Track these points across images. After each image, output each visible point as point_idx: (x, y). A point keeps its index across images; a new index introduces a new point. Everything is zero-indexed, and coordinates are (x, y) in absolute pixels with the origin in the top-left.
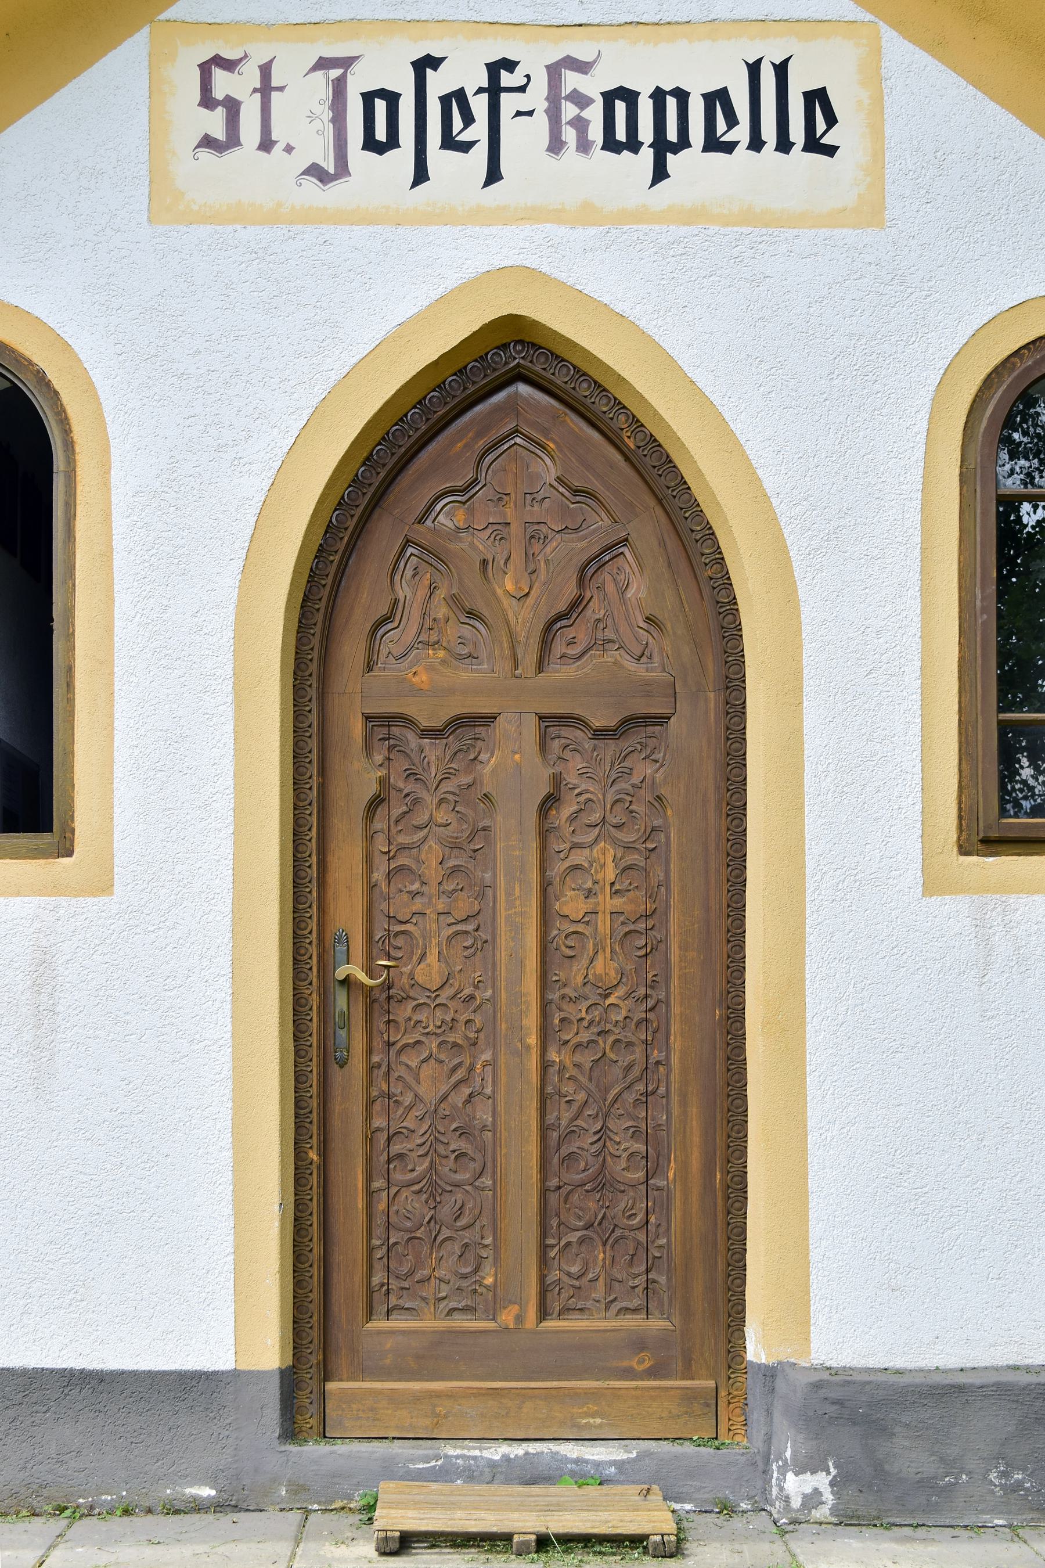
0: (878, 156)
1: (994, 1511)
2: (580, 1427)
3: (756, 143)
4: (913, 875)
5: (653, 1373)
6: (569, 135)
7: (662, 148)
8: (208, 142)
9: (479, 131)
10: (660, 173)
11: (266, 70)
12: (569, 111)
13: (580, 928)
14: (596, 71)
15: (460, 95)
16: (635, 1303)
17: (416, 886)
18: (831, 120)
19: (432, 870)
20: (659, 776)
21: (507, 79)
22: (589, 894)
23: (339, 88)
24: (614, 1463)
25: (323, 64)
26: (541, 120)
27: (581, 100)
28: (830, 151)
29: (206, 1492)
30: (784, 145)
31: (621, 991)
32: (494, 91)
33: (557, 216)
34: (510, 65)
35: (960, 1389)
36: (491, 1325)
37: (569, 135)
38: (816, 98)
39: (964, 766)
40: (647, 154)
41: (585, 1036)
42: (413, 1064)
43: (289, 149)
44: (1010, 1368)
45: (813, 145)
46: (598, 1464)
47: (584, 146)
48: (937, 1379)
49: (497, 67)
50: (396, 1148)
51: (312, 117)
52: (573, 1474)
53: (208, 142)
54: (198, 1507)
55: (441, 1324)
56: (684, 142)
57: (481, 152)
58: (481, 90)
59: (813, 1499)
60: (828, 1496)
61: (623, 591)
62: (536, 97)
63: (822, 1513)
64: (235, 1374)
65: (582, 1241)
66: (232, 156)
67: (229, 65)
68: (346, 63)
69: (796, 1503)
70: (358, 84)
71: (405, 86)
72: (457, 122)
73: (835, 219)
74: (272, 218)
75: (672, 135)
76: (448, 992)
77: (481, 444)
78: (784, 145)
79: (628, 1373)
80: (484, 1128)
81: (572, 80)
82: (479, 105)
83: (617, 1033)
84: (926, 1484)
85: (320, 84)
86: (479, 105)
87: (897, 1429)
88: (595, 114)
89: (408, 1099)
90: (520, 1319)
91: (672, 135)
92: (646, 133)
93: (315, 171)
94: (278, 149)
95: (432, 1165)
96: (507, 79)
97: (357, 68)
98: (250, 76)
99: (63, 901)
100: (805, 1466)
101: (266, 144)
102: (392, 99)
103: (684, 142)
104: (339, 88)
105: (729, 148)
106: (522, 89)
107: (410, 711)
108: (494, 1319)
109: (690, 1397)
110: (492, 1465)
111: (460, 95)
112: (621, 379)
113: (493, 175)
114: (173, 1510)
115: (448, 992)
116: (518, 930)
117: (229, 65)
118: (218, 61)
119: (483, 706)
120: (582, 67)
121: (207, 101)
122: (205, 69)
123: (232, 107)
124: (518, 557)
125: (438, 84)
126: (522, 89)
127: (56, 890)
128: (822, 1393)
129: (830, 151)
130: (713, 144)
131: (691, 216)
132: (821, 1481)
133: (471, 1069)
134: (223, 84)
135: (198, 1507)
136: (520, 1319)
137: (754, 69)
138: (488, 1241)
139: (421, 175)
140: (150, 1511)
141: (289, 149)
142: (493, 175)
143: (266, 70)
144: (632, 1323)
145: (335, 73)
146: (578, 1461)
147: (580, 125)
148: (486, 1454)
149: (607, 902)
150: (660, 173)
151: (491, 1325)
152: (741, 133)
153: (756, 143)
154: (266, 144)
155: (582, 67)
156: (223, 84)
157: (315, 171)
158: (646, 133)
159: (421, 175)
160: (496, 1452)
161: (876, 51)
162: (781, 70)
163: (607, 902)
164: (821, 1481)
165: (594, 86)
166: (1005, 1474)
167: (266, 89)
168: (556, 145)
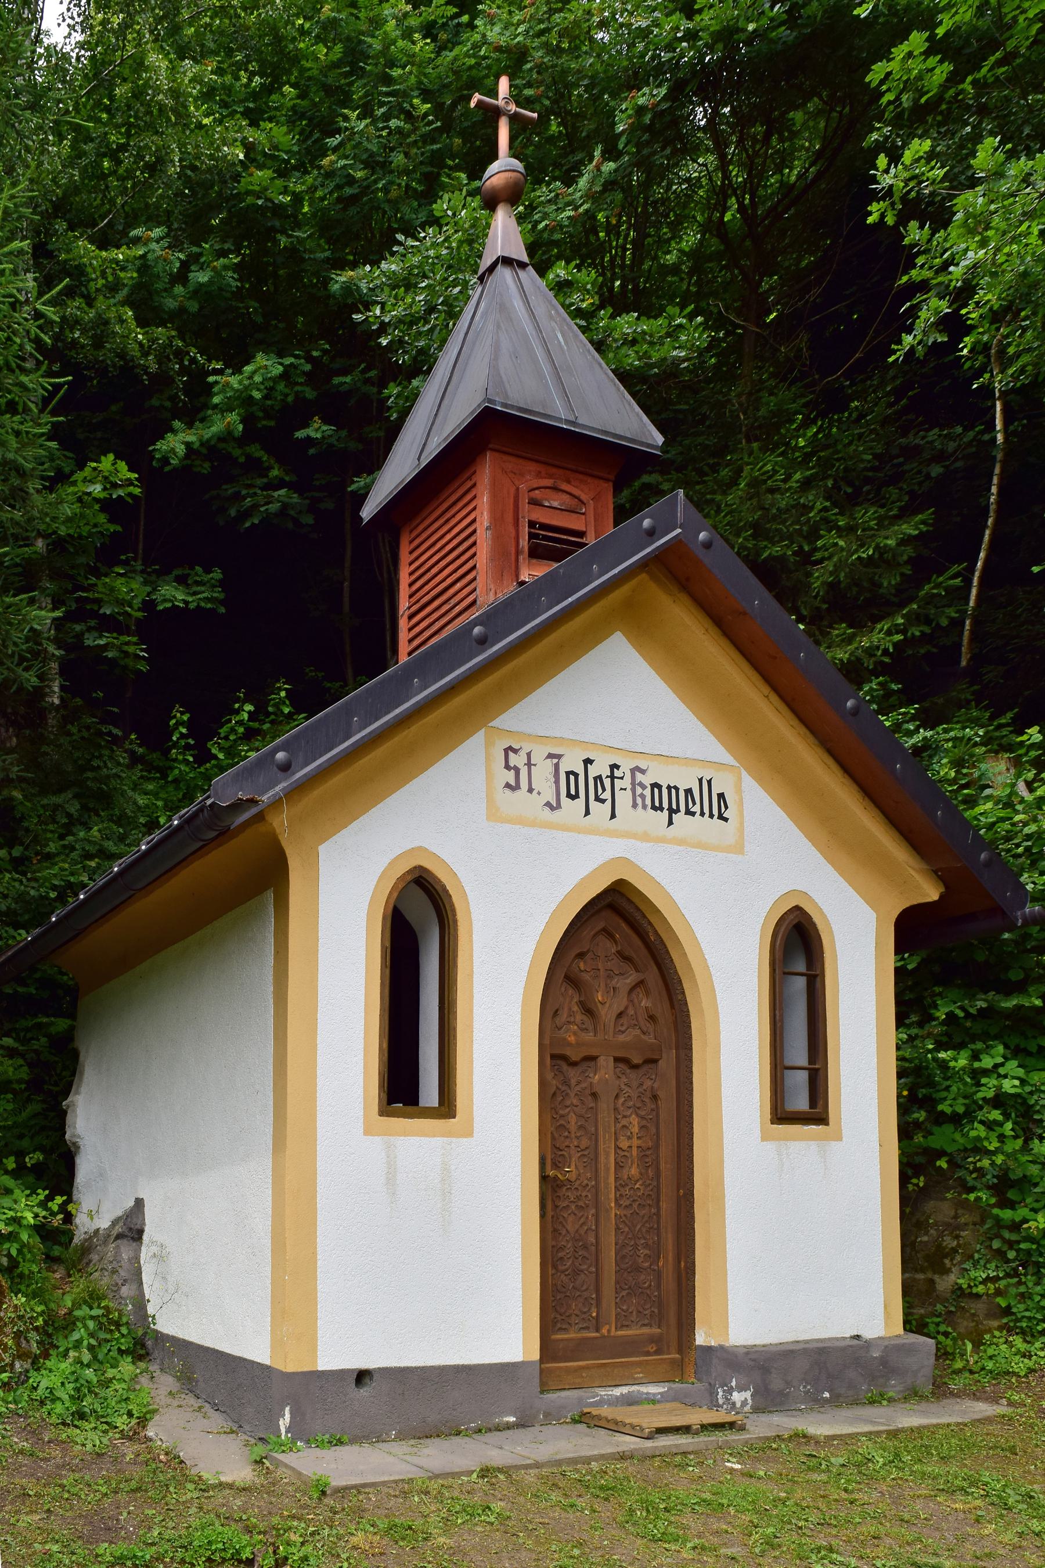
0: (742, 823)
1: (802, 1403)
2: (635, 1379)
3: (702, 814)
4: (757, 1132)
5: (658, 1352)
6: (639, 801)
7: (672, 811)
8: (508, 786)
9: (607, 795)
10: (670, 823)
11: (529, 755)
12: (639, 790)
13: (626, 1153)
14: (648, 773)
15: (600, 777)
16: (646, 1322)
17: (566, 1134)
18: (726, 807)
19: (573, 1126)
20: (656, 1085)
21: (617, 773)
22: (629, 1138)
23: (557, 767)
24: (659, 1393)
25: (550, 756)
26: (629, 792)
27: (641, 785)
28: (726, 820)
29: (512, 1419)
30: (711, 816)
31: (640, 1182)
32: (612, 777)
33: (634, 836)
34: (617, 767)
35: (792, 1351)
36: (597, 1335)
37: (639, 801)
38: (721, 796)
39: (549, 1076)
40: (666, 812)
41: (628, 1203)
42: (565, 1215)
43: (539, 793)
44: (792, 1342)
45: (721, 817)
46: (654, 1394)
47: (644, 807)
48: (782, 1348)
49: (614, 767)
50: (560, 1255)
51: (547, 780)
52: (646, 1399)
53: (508, 786)
54: (509, 1427)
55: (579, 1335)
56: (678, 810)
57: (609, 803)
58: (607, 777)
59: (744, 1403)
60: (750, 1401)
61: (640, 1003)
62: (626, 783)
63: (747, 1408)
64: (523, 1363)
65: (628, 1294)
66: (518, 793)
67: (515, 751)
68: (559, 757)
69: (738, 1405)
70: (563, 768)
71: (580, 769)
72: (600, 791)
73: (728, 849)
74: (533, 824)
75: (674, 807)
76: (578, 1182)
77: (593, 933)
78: (711, 816)
79: (648, 1354)
80: (592, 1244)
81: (639, 777)
82: (607, 782)
83: (640, 1201)
84: (781, 1393)
85: (550, 764)
86: (607, 782)
87: (773, 1370)
88: (647, 792)
89: (564, 1232)
90: (609, 1331)
91: (674, 807)
92: (665, 805)
93: (548, 804)
94: (535, 792)
95: (573, 1262)
96: (617, 773)
97: (563, 759)
99: (454, 1140)
100: (741, 1389)
101: (530, 790)
102: (576, 775)
103: (678, 810)
104: (557, 767)
105: (693, 814)
106: (622, 778)
107: (568, 1053)
108: (597, 1331)
109: (673, 1362)
110: (617, 1397)
111: (600, 777)
112: (658, 911)
113: (613, 816)
114: (498, 1429)
115: (578, 1182)
116: (607, 1154)
117: (515, 751)
118: (510, 748)
119: (594, 1052)
120: (643, 772)
121: (507, 767)
122: (507, 750)
123: (517, 770)
124: (602, 985)
125: (593, 772)
126: (622, 778)
127: (449, 1134)
128: (750, 1356)
129: (726, 820)
130: (688, 812)
131: (681, 842)
132: (747, 1395)
133: (587, 1218)
134: (514, 760)
135: (509, 1427)
136: (609, 1331)
137: (700, 780)
138: (594, 1296)
139: (587, 812)
140: (490, 1430)
141: (539, 793)
142: (613, 816)
143: (529, 755)
144: (646, 1330)
145: (555, 761)
146: (647, 1393)
147: (642, 796)
148: (614, 1393)
149: (635, 1142)
150: (670, 823)
151: (597, 1335)
152: (697, 808)
153: (702, 814)
154: (530, 790)
155: (643, 772)
156: (514, 760)
157: (548, 804)
158: (665, 805)
159: (587, 812)
160: (617, 1392)
161: (740, 779)
162: (709, 782)
163: (635, 1142)
164: (747, 1395)
165: (647, 780)
166: (805, 1387)
167: (529, 764)
168: (635, 805)
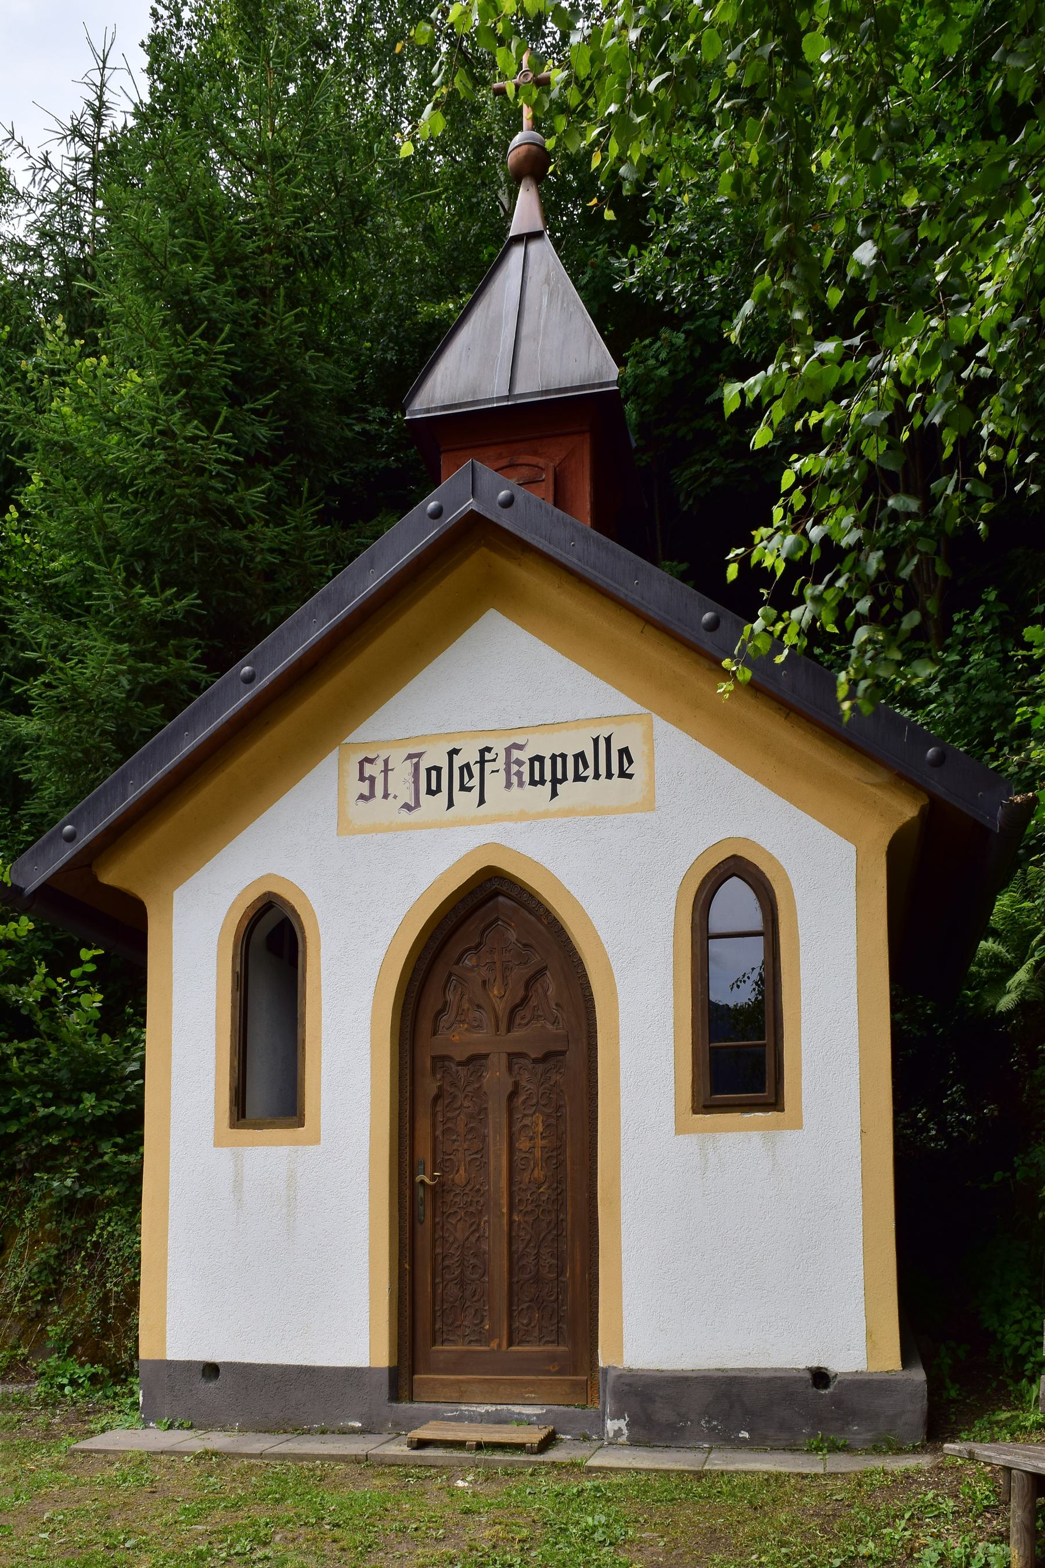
1: (704, 1440)
3: (597, 776)
6: (515, 779)
7: (555, 781)
8: (362, 797)
9: (475, 782)
10: (554, 794)
11: (386, 762)
12: (515, 768)
14: (526, 748)
17: (454, 1137)
18: (631, 762)
21: (488, 756)
22: (531, 1139)
25: (410, 757)
26: (502, 774)
27: (519, 763)
28: (630, 776)
30: (609, 776)
32: (482, 762)
33: (510, 818)
34: (488, 749)
37: (515, 779)
38: (624, 752)
41: (530, 1208)
42: (454, 1222)
43: (395, 797)
45: (623, 774)
46: (528, 1415)
47: (521, 784)
49: (482, 752)
50: (446, 1263)
51: (405, 781)
52: (517, 1420)
53: (362, 797)
56: (565, 778)
57: (476, 791)
58: (476, 762)
59: (618, 1433)
60: (625, 1431)
62: (500, 763)
63: (623, 1439)
64: (370, 1369)
65: (528, 1308)
66: (373, 801)
67: (371, 761)
68: (419, 755)
74: (388, 829)
75: (559, 776)
76: (469, 1187)
77: (482, 925)
78: (609, 776)
80: (484, 1253)
81: (516, 754)
82: (476, 769)
85: (409, 765)
86: (476, 769)
88: (526, 769)
89: (451, 1239)
91: (559, 776)
92: (548, 776)
93: (407, 807)
94: (391, 797)
95: (462, 1272)
97: (424, 757)
98: (380, 765)
99: (300, 1147)
101: (386, 796)
102: (438, 770)
105: (585, 779)
106: (494, 760)
109: (574, 1384)
110: (481, 1414)
111: (467, 766)
113: (482, 801)
115: (469, 1187)
117: (371, 761)
120: (520, 747)
121: (362, 778)
122: (361, 764)
123: (372, 780)
124: (499, 980)
125: (458, 761)
126: (494, 760)
127: (297, 1142)
128: (622, 1380)
129: (630, 776)
130: (578, 778)
132: (622, 1424)
133: (479, 1224)
134: (368, 770)
136: (499, 1346)
137: (596, 741)
139: (451, 804)
142: (482, 801)
143: (386, 762)
144: (550, 1348)
145: (415, 760)
146: (519, 1414)
147: (519, 774)
148: (479, 1410)
149: (540, 1142)
150: (554, 794)
152: (590, 772)
153: (597, 776)
155: (520, 747)
156: (368, 770)
157: (407, 807)
158: (548, 776)
159: (451, 804)
160: (482, 1409)
161: (651, 727)
162: (608, 740)
163: (540, 1142)
164: (622, 1424)
165: (524, 756)
166: (707, 1422)
167: (386, 771)
168: (509, 785)
